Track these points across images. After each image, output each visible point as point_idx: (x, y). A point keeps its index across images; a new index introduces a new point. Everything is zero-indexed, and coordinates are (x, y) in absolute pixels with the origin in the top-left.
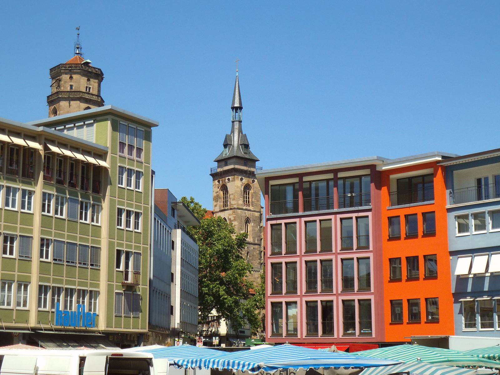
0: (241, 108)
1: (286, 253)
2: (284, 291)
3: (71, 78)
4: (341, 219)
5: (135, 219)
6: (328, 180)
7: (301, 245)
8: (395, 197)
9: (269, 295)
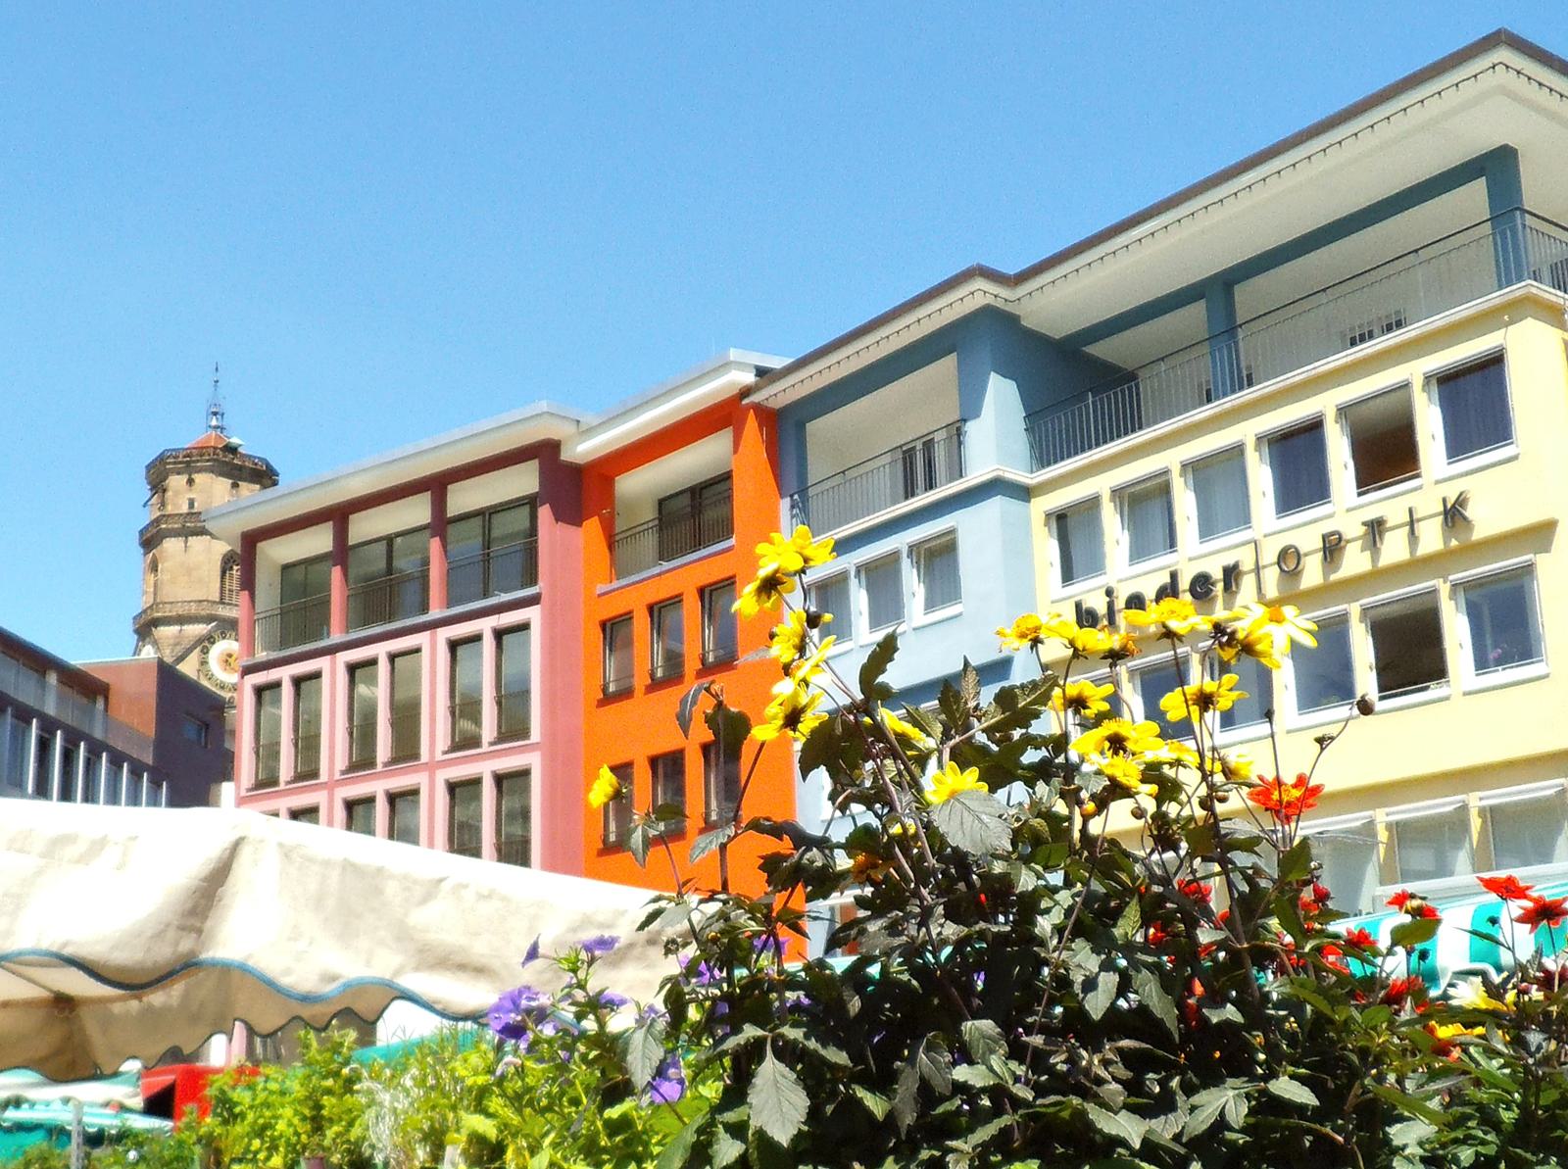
3: (190, 482)
4: (454, 646)
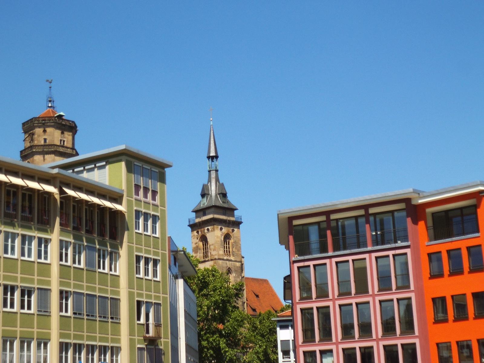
0: (217, 157)
1: (317, 297)
2: (317, 338)
3: (45, 131)
5: (154, 267)
6: (356, 218)
7: (333, 289)
8: (432, 231)
9: (300, 344)
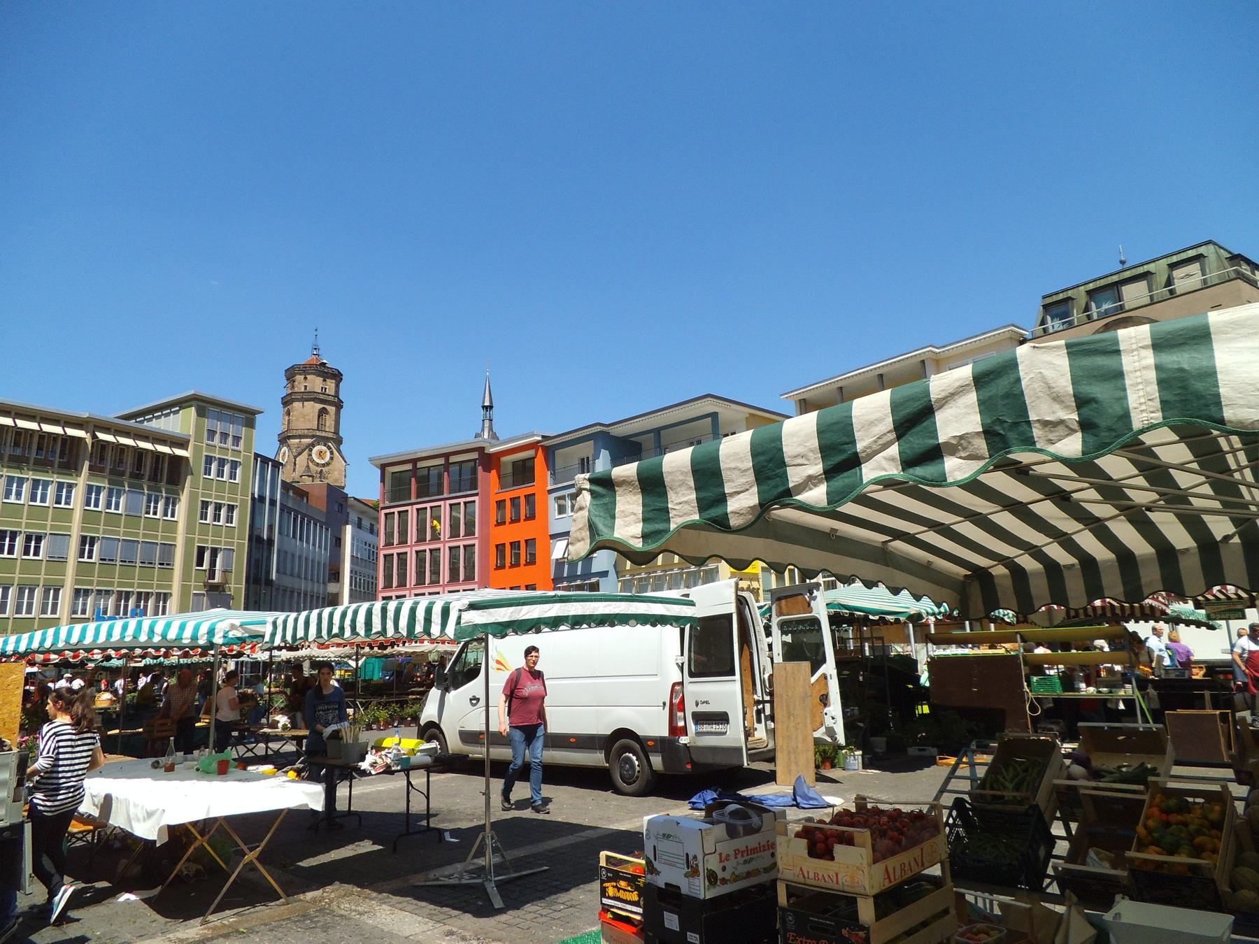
4: (451, 505)
